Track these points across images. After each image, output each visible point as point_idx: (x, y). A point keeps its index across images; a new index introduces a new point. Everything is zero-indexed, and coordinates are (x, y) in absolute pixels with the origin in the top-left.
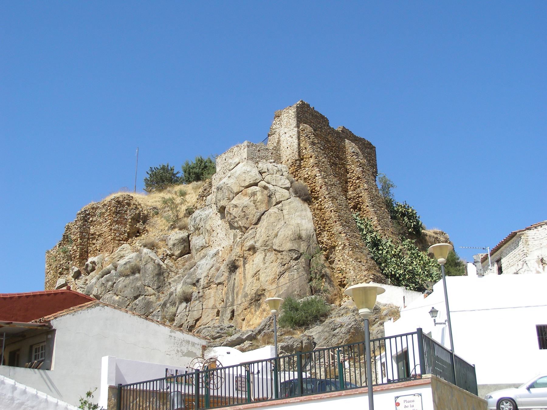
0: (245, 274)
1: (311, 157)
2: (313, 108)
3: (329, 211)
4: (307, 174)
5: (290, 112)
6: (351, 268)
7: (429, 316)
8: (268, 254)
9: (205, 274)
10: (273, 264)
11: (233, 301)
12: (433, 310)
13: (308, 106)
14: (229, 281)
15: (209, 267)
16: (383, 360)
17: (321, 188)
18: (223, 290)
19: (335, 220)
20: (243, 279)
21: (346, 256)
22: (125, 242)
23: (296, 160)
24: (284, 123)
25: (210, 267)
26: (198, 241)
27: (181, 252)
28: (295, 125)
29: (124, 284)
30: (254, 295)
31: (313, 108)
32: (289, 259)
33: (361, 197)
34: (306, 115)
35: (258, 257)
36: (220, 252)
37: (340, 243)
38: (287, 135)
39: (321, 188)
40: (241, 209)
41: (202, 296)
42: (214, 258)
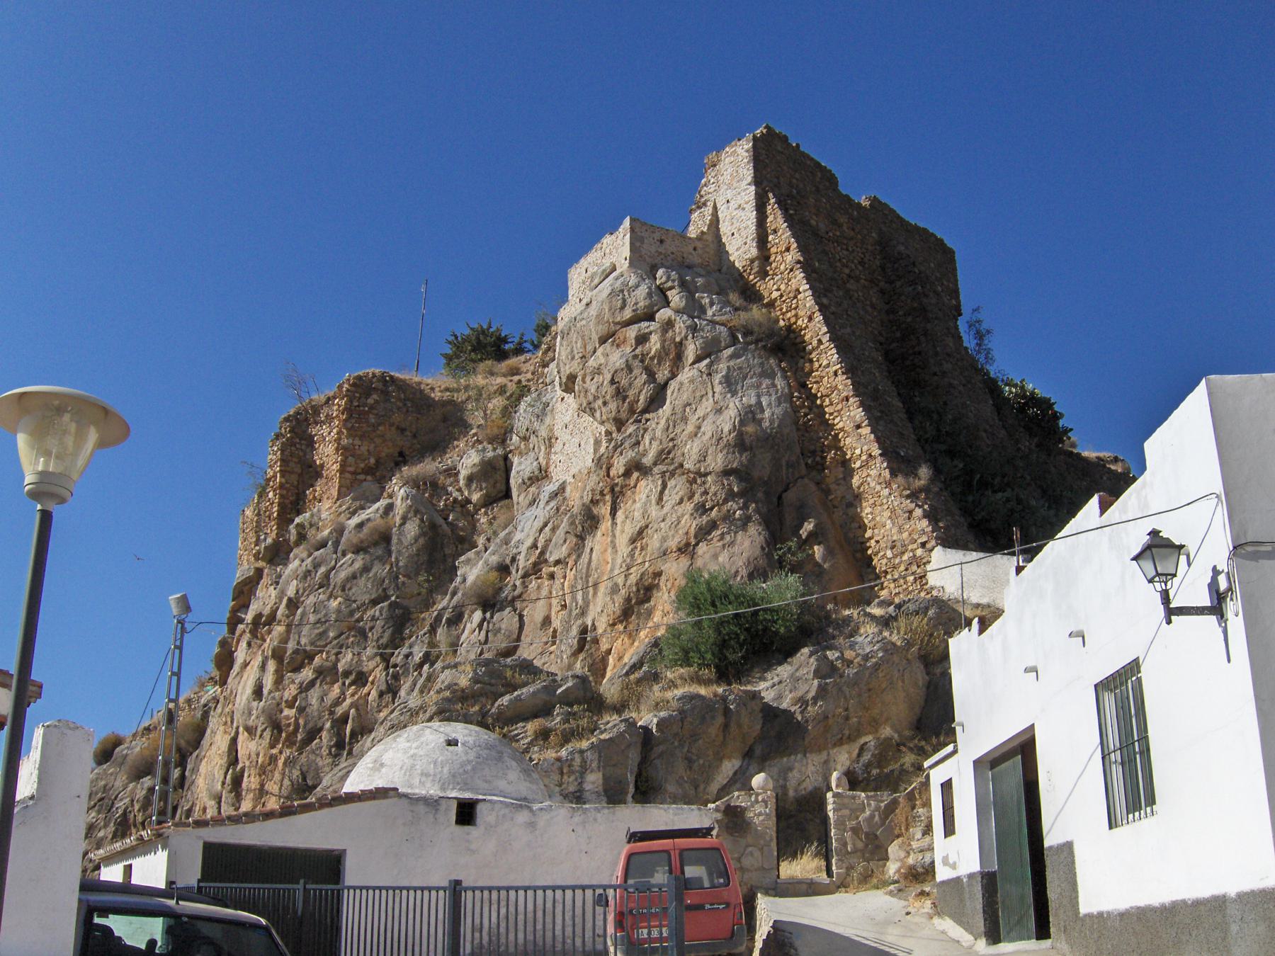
0: (614, 536)
1: (788, 249)
2: (798, 145)
3: (831, 374)
4: (778, 290)
5: (739, 150)
6: (887, 514)
7: (1136, 575)
8: (671, 483)
9: (529, 542)
10: (680, 509)
11: (587, 604)
12: (1157, 541)
13: (785, 139)
14: (579, 556)
15: (538, 524)
16: (599, 910)
17: (810, 319)
18: (565, 577)
19: (845, 394)
20: (610, 550)
21: (872, 484)
22: (369, 478)
23: (752, 261)
24: (726, 177)
25: (541, 524)
26: (523, 467)
27: (487, 495)
28: (749, 179)
29: (351, 570)
30: (634, 589)
31: (798, 145)
32: (722, 496)
33: (920, 353)
34: (786, 176)
35: (645, 489)
36: (568, 489)
37: (858, 452)
38: (733, 205)
39: (810, 319)
40: (609, 377)
41: (520, 596)
42: (552, 504)
